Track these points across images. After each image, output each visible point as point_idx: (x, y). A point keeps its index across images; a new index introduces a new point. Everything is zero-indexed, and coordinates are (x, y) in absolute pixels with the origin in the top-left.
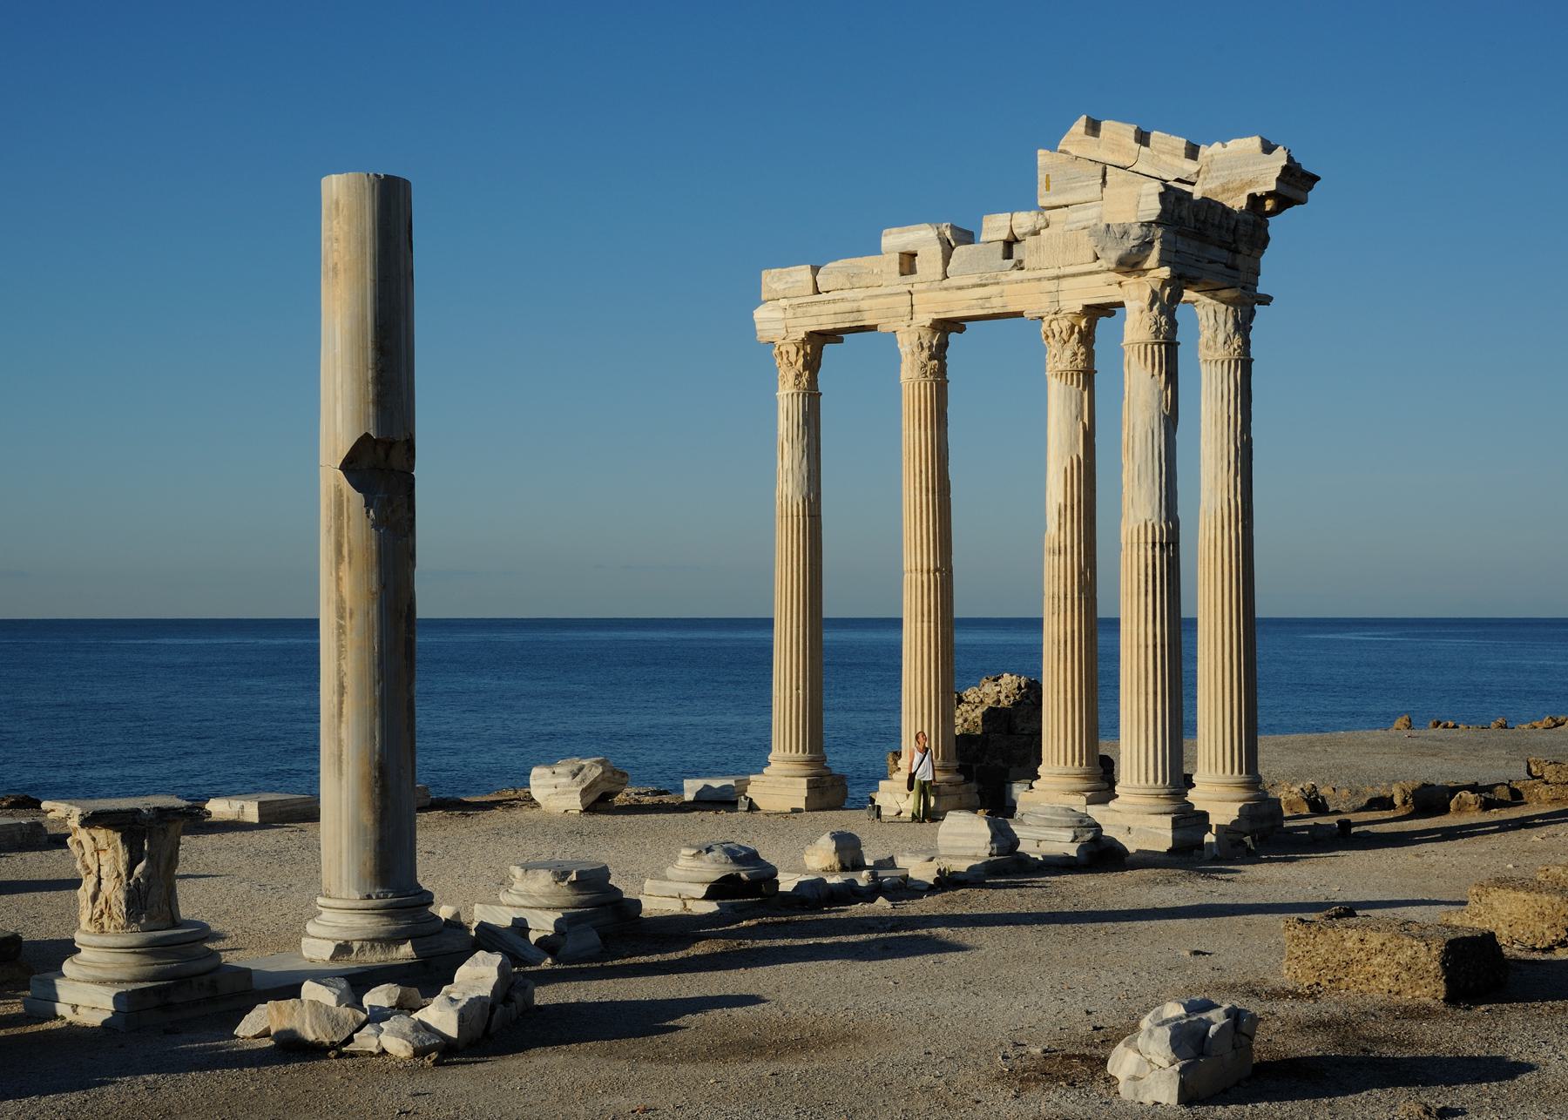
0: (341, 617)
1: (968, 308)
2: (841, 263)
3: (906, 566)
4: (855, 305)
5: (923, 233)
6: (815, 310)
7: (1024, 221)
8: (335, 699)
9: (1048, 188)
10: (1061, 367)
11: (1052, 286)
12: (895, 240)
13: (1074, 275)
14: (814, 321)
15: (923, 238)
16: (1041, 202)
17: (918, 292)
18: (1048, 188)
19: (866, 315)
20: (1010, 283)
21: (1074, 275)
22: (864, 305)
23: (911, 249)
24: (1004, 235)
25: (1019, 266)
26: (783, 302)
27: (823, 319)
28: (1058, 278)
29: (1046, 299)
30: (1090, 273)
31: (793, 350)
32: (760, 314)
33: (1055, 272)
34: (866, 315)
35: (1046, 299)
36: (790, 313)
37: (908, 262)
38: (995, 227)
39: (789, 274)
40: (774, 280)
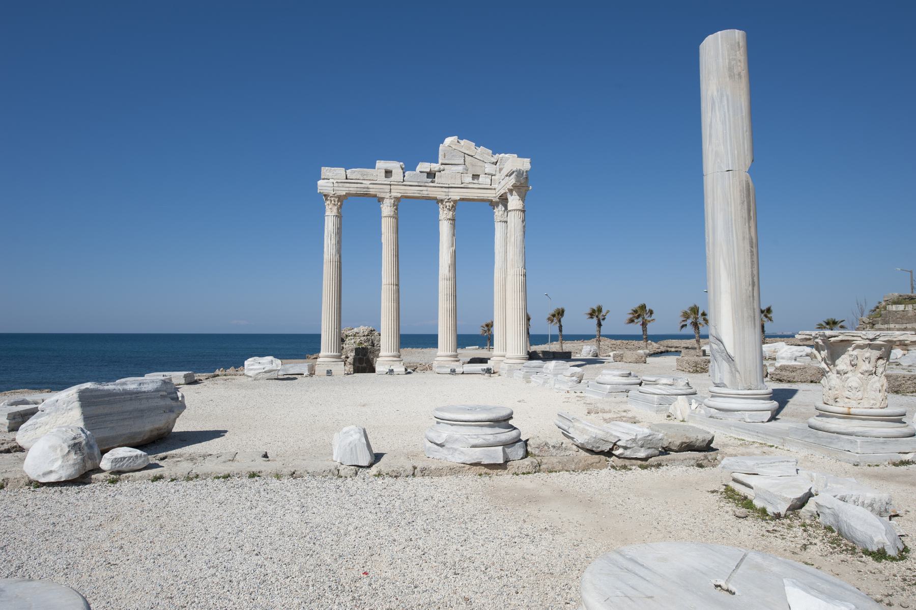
0: (752, 247)
6: (348, 185)
7: (435, 167)
8: (750, 288)
12: (382, 165)
15: (395, 166)
24: (428, 170)
25: (432, 182)
32: (320, 182)
36: (336, 185)
37: (388, 173)
38: (424, 167)
40: (326, 171)
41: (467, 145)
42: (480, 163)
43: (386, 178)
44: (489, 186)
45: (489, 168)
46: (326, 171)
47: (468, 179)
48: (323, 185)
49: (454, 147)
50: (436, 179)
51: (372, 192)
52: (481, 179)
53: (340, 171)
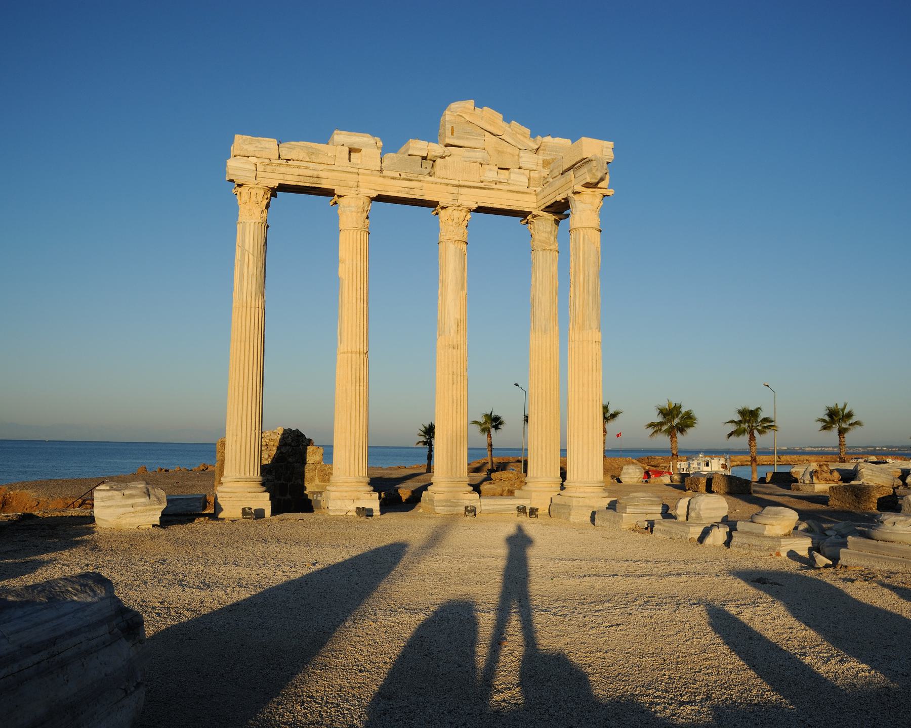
1: (398, 191)
2: (301, 143)
3: (342, 347)
4: (315, 173)
5: (365, 139)
7: (436, 149)
9: (452, 134)
10: (457, 238)
11: (455, 190)
13: (470, 187)
14: (281, 176)
16: (448, 141)
17: (364, 174)
18: (452, 134)
19: (323, 181)
20: (428, 182)
21: (470, 187)
22: (322, 174)
23: (356, 146)
26: (254, 160)
27: (287, 177)
28: (460, 186)
29: (451, 197)
30: (477, 188)
31: (261, 192)
33: (456, 183)
34: (323, 181)
35: (451, 197)
38: (419, 147)
39: (258, 141)
40: (241, 143)
41: (489, 117)
42: (510, 149)
43: (355, 164)
44: (526, 190)
45: (528, 159)
46: (241, 143)
47: (491, 174)
48: (236, 167)
49: (468, 118)
50: (438, 170)
51: (325, 185)
52: (513, 176)
53: (270, 144)
